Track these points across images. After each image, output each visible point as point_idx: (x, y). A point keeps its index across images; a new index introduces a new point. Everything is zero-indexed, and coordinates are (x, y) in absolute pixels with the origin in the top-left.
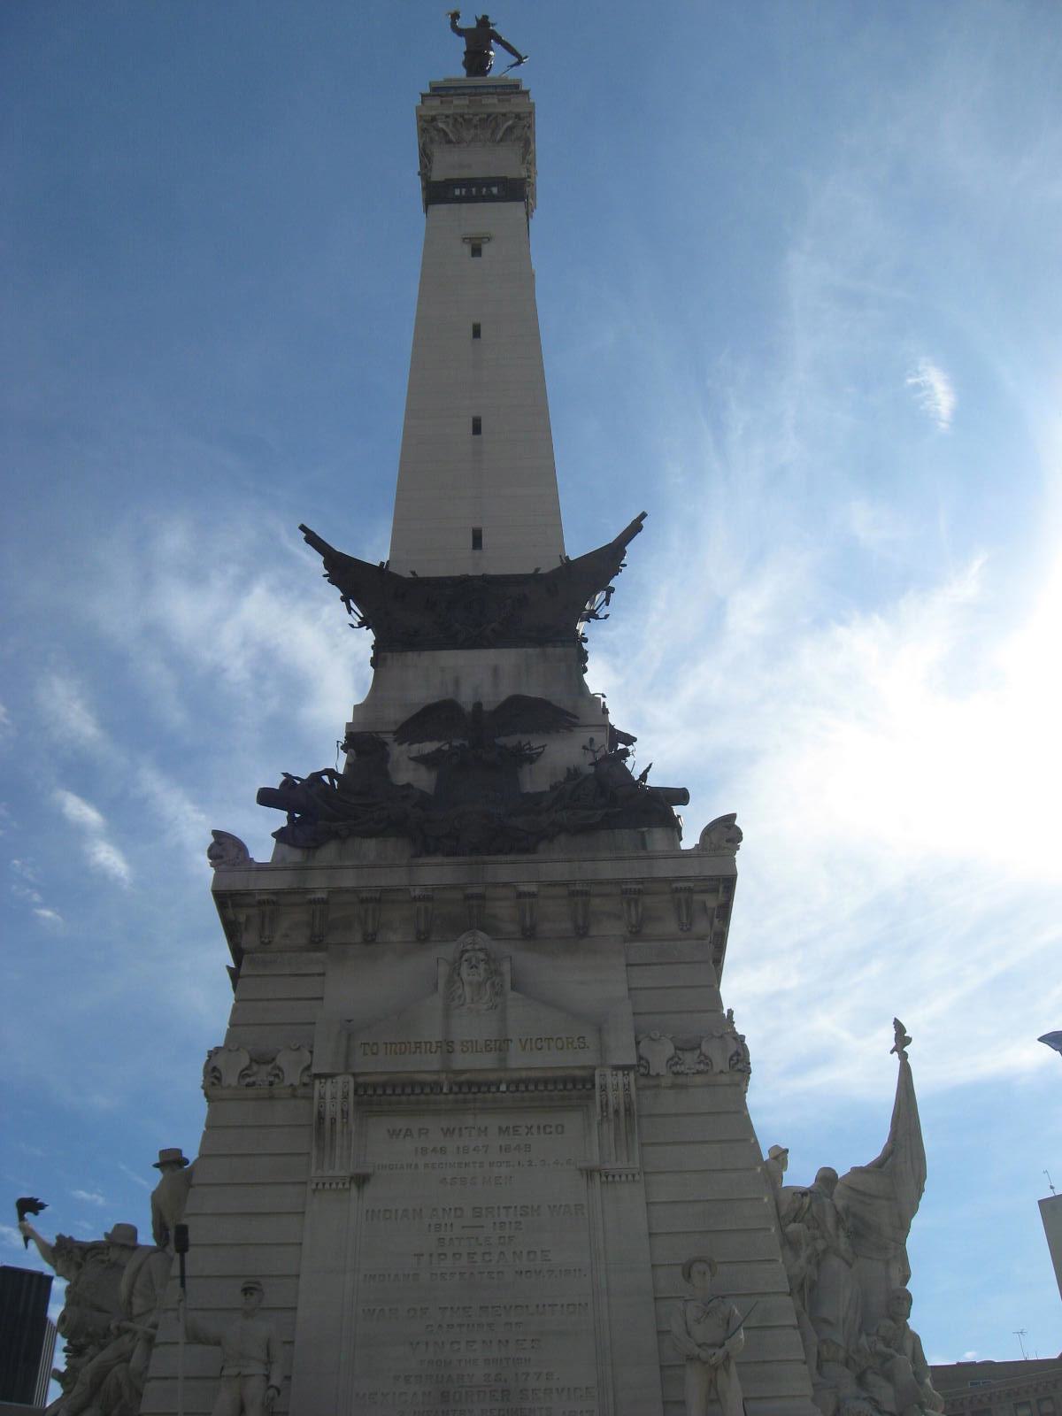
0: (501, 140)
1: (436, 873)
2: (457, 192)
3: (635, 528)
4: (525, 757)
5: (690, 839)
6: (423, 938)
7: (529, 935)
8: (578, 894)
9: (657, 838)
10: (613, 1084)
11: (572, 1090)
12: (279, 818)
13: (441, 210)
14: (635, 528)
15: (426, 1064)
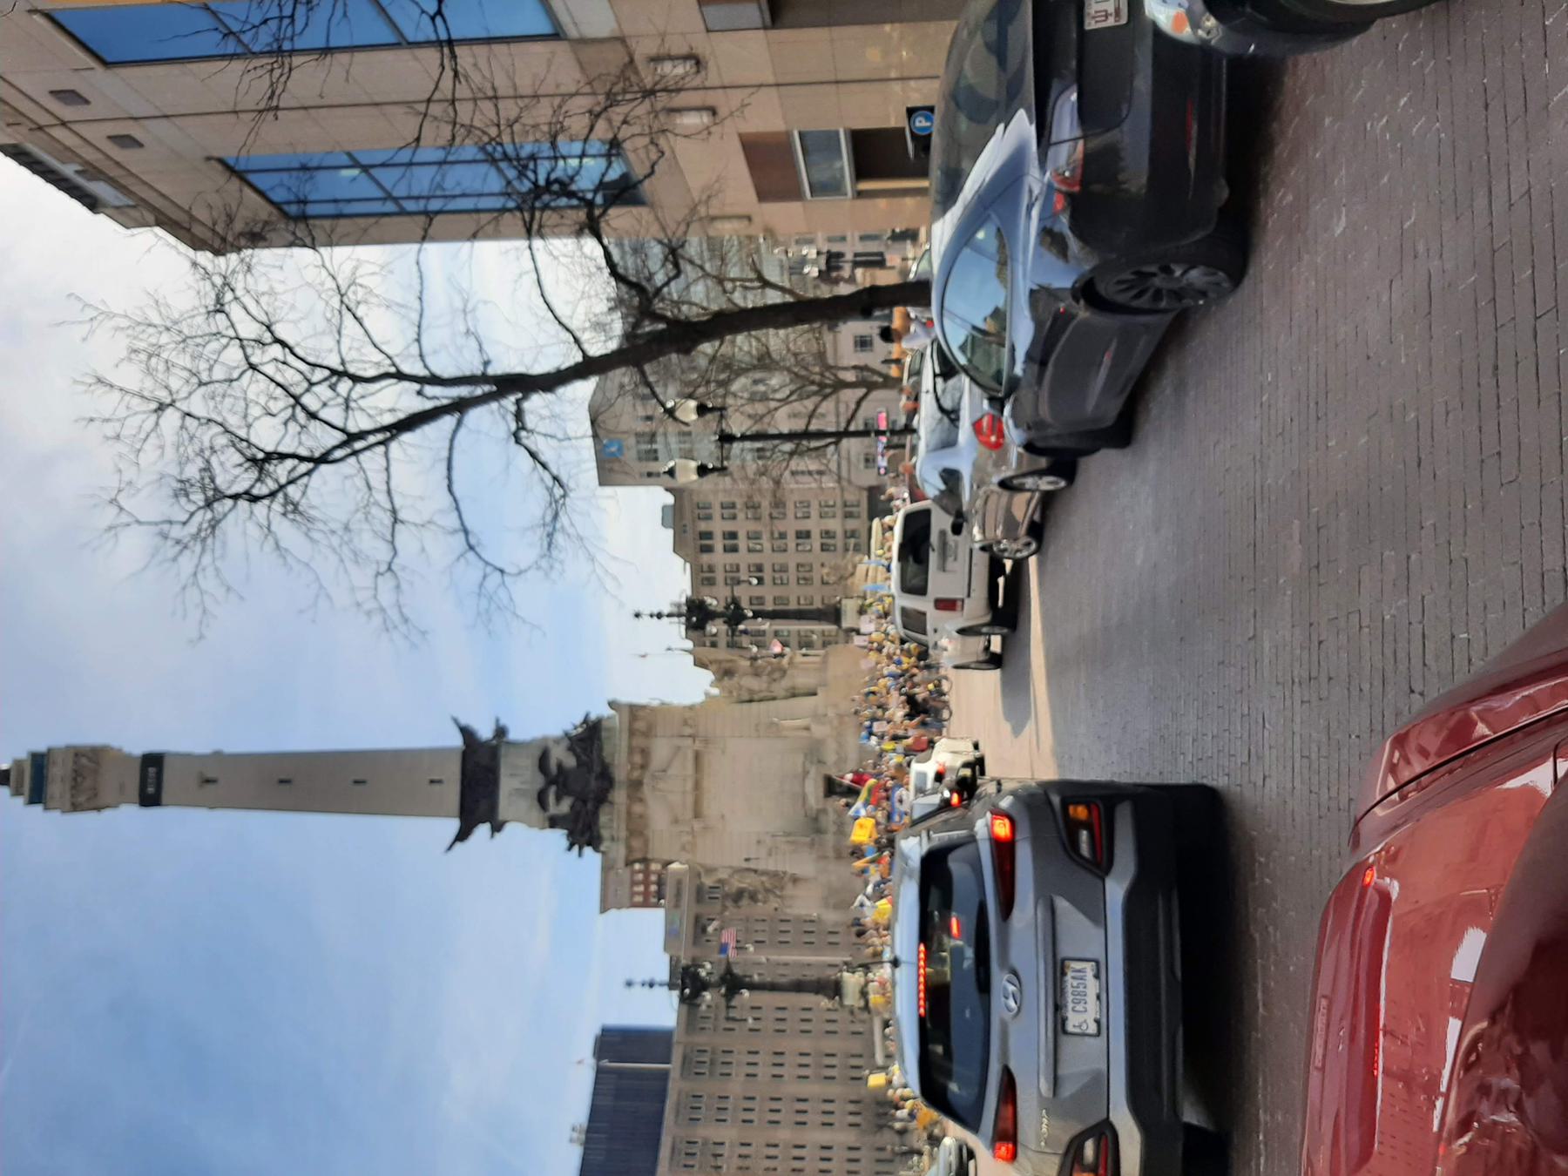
0: (98, 763)
1: (619, 796)
2: (151, 790)
3: (456, 721)
4: (560, 766)
5: (612, 712)
6: (641, 800)
7: (644, 767)
8: (631, 750)
9: (604, 724)
10: (698, 745)
11: (698, 757)
12: (588, 850)
13: (165, 797)
14: (456, 721)
15: (690, 799)
